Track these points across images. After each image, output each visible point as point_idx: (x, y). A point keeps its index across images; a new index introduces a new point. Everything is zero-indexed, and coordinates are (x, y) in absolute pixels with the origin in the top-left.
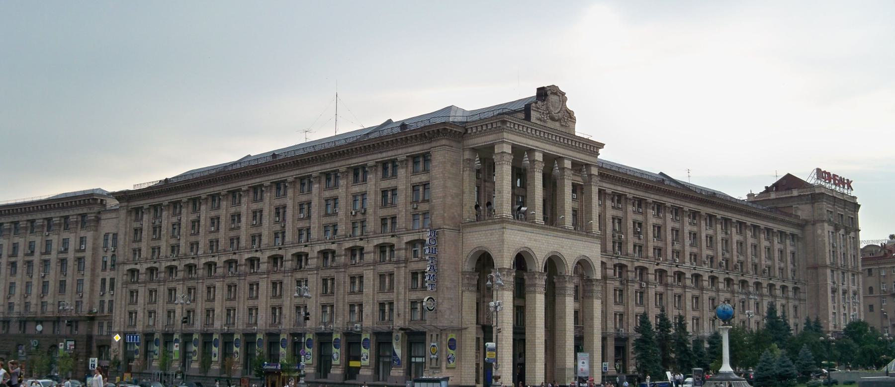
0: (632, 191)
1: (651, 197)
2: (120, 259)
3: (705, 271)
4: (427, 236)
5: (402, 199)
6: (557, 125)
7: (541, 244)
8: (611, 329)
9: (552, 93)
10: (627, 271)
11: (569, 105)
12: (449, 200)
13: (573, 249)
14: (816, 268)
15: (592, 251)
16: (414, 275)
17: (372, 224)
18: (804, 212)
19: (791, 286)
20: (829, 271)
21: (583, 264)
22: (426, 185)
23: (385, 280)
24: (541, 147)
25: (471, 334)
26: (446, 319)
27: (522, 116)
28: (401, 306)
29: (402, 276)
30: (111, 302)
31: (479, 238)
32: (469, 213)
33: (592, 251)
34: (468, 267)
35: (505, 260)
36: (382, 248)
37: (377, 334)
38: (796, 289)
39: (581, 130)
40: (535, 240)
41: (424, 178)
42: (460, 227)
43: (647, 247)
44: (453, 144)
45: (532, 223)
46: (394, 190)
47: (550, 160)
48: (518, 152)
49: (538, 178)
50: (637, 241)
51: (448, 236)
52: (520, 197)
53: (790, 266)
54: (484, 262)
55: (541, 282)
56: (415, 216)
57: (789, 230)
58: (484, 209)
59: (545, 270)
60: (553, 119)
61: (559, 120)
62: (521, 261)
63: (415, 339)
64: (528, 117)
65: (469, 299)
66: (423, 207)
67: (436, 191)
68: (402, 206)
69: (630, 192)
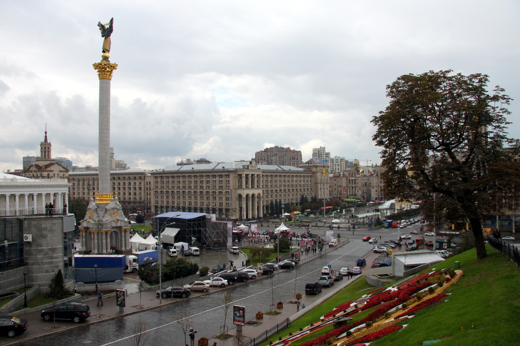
1: (274, 174)
2: (151, 188)
3: (287, 188)
4: (229, 191)
5: (224, 183)
7: (250, 192)
8: (265, 204)
13: (256, 192)
14: (316, 183)
16: (227, 198)
17: (217, 187)
18: (314, 170)
19: (309, 188)
20: (319, 185)
21: (259, 194)
22: (229, 181)
23: (221, 198)
24: (250, 173)
25: (238, 208)
26: (234, 206)
27: (247, 167)
28: (224, 204)
29: (224, 198)
30: (150, 198)
31: (240, 192)
32: (237, 187)
34: (237, 197)
35: (244, 196)
36: (220, 192)
37: (219, 209)
38: (311, 189)
41: (228, 179)
42: (236, 189)
45: (249, 188)
46: (222, 181)
48: (247, 175)
49: (250, 179)
51: (234, 191)
52: (247, 183)
53: (310, 183)
54: (240, 196)
55: (251, 199)
56: (226, 186)
57: (309, 175)
58: (240, 187)
62: (247, 195)
63: (227, 210)
64: (248, 168)
65: (238, 202)
66: (228, 185)
67: (231, 182)
68: (224, 184)
69: (269, 174)
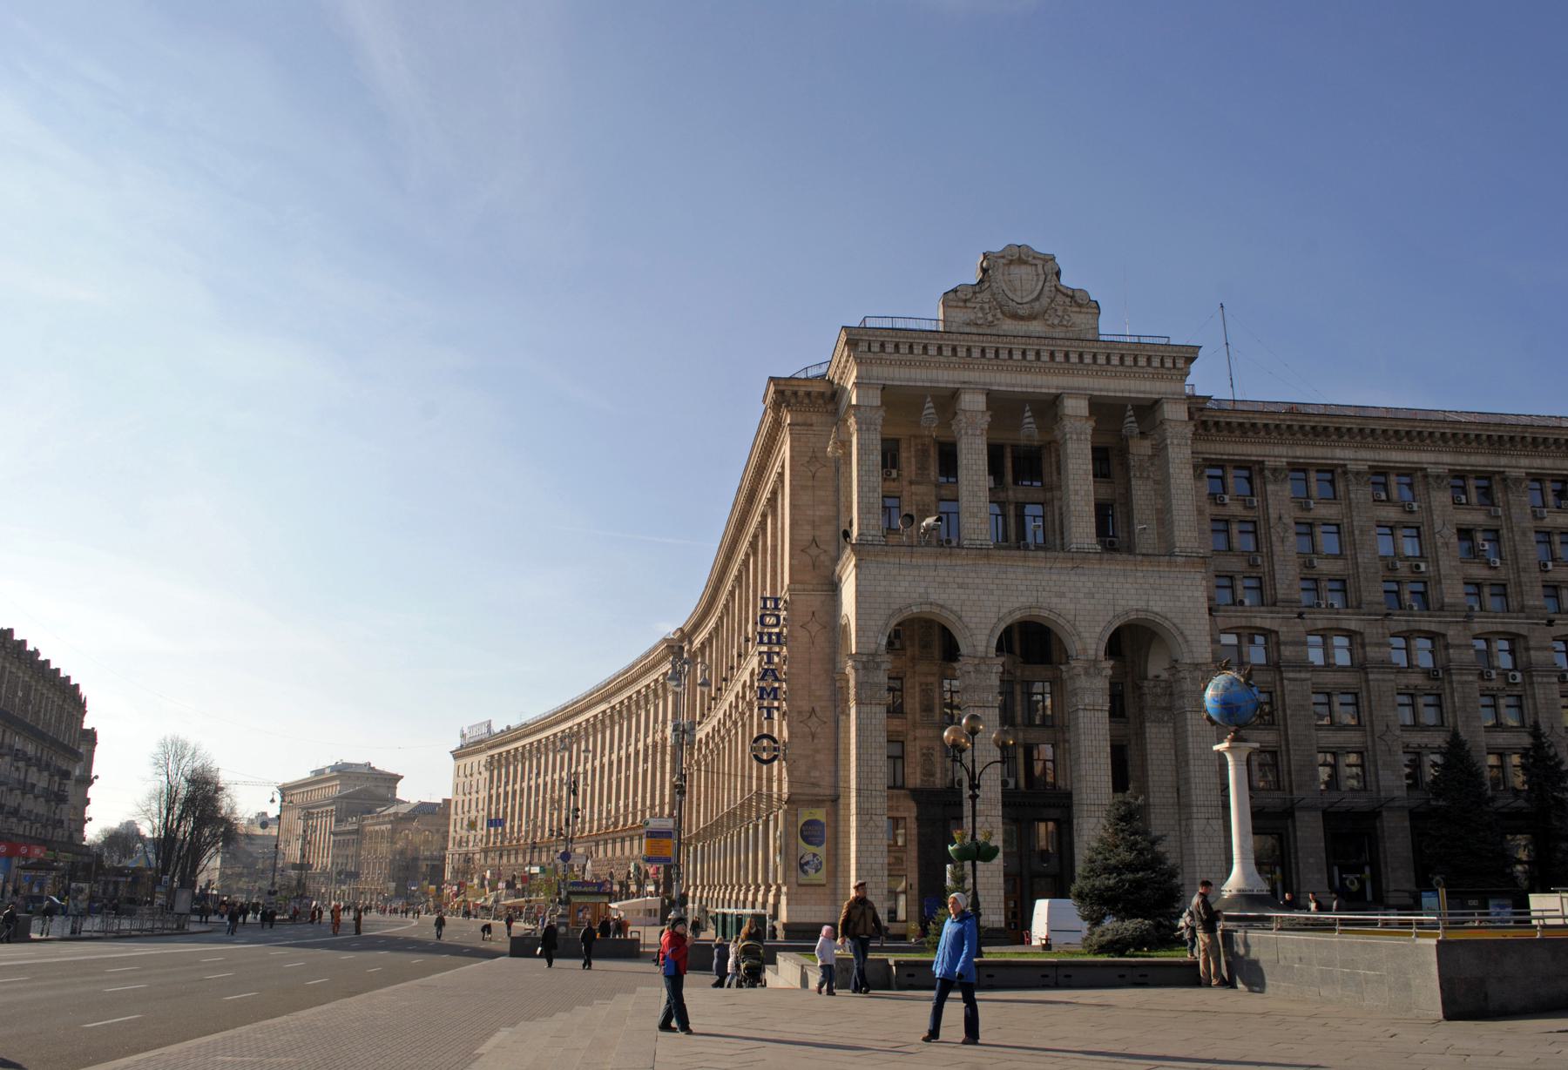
0: (1447, 458)
6: (1036, 327)
9: (1011, 262)
10: (1447, 647)
11: (1065, 281)
12: (806, 533)
15: (1178, 599)
33: (1178, 599)
39: (1113, 325)
40: (960, 586)
43: (1519, 584)
44: (814, 418)
47: (1003, 406)
50: (1478, 572)
59: (999, 649)
60: (1015, 316)
61: (1032, 317)
